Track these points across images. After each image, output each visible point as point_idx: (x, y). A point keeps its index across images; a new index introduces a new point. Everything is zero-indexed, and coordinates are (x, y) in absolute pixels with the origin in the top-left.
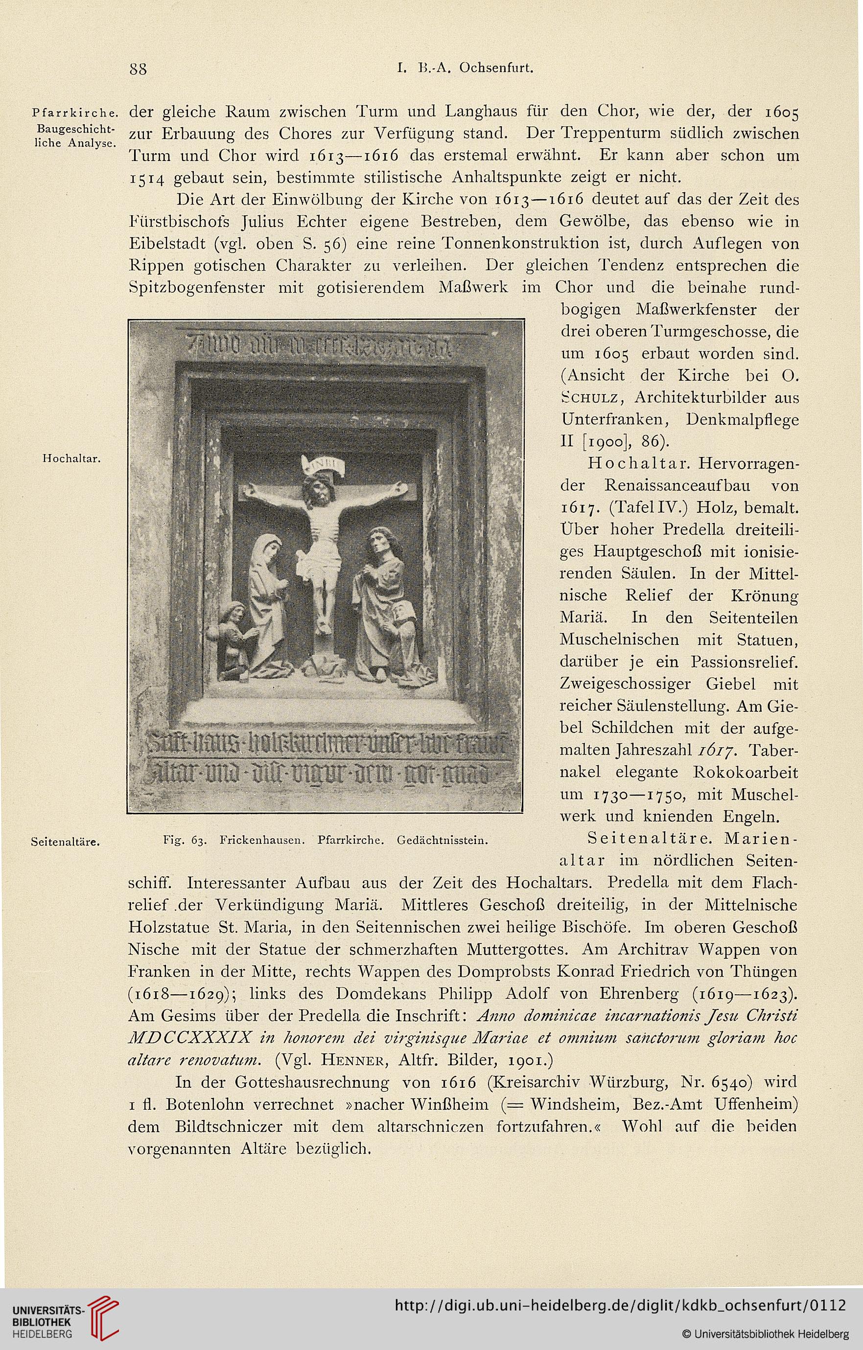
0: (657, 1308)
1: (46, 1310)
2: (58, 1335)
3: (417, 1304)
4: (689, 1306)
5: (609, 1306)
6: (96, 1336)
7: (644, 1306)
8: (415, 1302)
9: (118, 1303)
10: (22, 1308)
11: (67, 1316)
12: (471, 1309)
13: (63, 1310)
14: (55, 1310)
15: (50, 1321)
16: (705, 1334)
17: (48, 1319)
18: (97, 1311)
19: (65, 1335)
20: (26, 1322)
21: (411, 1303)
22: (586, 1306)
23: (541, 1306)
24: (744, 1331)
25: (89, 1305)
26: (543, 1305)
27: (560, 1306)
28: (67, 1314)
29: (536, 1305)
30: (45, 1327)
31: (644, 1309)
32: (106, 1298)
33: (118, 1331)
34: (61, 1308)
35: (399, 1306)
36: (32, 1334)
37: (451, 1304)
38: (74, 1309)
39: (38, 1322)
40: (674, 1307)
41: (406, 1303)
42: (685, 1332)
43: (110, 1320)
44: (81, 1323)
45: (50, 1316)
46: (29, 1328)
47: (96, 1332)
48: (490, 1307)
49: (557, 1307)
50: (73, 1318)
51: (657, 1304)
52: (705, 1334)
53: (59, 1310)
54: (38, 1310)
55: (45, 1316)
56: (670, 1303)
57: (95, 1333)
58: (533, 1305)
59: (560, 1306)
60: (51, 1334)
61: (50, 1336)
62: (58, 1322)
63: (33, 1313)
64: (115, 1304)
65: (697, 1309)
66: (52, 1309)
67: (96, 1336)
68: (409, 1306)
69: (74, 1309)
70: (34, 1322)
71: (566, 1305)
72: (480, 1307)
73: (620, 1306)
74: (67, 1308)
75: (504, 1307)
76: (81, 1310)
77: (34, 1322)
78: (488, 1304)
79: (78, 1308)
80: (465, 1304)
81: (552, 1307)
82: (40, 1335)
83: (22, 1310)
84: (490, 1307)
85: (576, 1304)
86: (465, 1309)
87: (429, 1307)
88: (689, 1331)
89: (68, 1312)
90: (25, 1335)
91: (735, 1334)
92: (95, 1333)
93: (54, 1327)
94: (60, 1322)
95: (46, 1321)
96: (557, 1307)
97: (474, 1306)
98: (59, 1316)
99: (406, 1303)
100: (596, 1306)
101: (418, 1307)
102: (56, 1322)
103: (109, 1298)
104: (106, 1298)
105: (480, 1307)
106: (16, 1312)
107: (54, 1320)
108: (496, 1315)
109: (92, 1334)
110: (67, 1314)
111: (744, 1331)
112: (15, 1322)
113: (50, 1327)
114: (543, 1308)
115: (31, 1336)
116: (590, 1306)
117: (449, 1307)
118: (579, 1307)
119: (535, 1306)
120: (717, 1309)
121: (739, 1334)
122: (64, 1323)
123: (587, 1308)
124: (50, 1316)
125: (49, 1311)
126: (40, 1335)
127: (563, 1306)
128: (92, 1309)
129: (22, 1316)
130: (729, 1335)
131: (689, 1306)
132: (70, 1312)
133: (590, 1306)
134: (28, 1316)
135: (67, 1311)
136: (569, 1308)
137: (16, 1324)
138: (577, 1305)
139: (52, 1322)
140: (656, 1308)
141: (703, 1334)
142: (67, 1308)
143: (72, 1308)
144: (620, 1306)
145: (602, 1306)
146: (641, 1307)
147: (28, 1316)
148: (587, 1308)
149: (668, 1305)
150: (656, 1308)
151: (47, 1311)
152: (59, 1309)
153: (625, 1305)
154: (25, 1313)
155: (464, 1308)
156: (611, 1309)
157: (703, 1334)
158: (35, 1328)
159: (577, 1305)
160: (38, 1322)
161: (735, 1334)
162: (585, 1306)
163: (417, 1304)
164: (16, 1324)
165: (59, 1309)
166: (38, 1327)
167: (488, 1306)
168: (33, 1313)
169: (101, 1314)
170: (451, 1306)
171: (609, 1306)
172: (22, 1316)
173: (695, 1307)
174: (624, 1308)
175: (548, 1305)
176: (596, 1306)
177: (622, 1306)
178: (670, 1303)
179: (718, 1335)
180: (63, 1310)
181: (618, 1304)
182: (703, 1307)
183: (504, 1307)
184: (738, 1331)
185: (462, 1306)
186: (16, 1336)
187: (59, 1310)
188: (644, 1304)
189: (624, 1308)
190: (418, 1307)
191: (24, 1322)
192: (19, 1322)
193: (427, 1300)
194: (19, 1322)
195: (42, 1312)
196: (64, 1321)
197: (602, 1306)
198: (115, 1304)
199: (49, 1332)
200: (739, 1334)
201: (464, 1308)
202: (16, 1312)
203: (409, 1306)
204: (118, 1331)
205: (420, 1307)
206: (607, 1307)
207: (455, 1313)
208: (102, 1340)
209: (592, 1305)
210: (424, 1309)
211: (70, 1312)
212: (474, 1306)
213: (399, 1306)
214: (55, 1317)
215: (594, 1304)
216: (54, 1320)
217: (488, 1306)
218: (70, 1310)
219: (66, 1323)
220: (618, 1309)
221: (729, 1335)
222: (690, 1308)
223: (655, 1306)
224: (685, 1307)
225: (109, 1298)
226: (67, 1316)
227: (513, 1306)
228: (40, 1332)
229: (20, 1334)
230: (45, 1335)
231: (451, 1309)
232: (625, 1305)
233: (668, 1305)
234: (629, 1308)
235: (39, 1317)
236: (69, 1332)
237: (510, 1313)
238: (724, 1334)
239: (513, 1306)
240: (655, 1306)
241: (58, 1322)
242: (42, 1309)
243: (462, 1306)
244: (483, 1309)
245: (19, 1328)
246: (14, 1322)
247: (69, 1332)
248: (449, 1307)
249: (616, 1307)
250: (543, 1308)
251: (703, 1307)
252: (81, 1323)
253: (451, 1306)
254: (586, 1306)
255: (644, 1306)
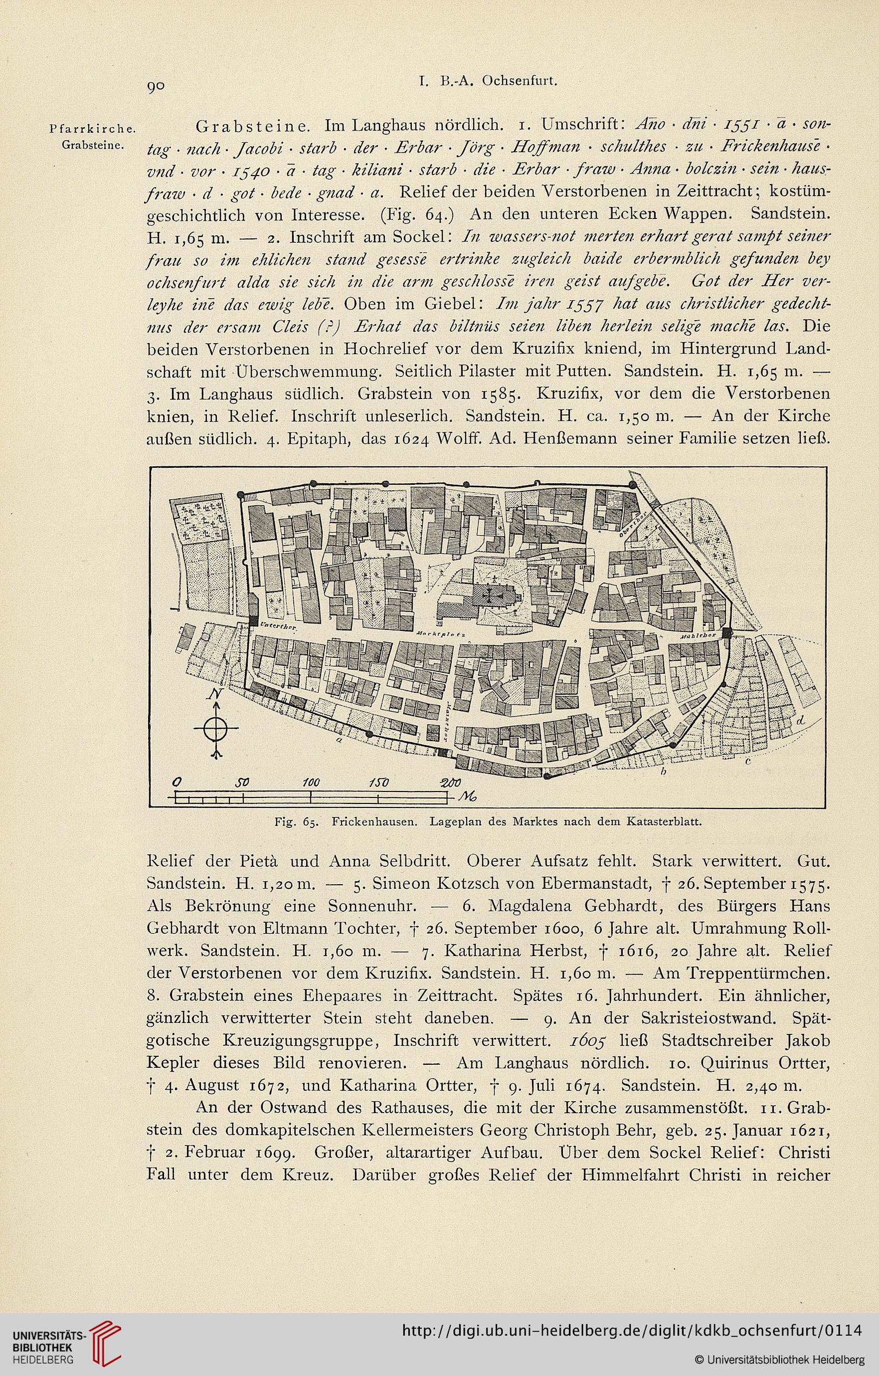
0: (670, 1334)
1: (46, 1335)
2: (59, 1361)
3: (425, 1329)
4: (702, 1332)
5: (620, 1331)
6: (98, 1362)
7: (656, 1331)
8: (423, 1327)
9: (120, 1329)
10: (22, 1333)
11: (68, 1341)
12: (480, 1334)
13: (65, 1335)
14: (56, 1335)
15: (51, 1347)
16: (718, 1360)
17: (49, 1345)
18: (99, 1336)
19: (66, 1360)
20: (27, 1348)
21: (419, 1328)
22: (597, 1331)
23: (551, 1331)
24: (758, 1357)
25: (90, 1330)
26: (553, 1330)
27: (570, 1331)
28: (68, 1339)
29: (546, 1330)
30: (46, 1352)
31: (656, 1334)
32: (108, 1323)
33: (120, 1357)
34: (62, 1333)
35: (407, 1331)
36: (33, 1360)
37: (460, 1329)
38: (76, 1334)
39: (38, 1347)
40: (686, 1332)
41: (413, 1328)
42: (697, 1357)
43: (112, 1346)
44: (82, 1349)
45: (50, 1342)
46: (29, 1353)
47: (98, 1358)
48: (499, 1332)
49: (567, 1332)
50: (74, 1343)
51: (670, 1329)
52: (718, 1360)
53: (60, 1335)
54: (39, 1336)
55: (46, 1341)
56: (683, 1328)
57: (96, 1359)
58: (543, 1330)
59: (570, 1331)
60: (52, 1360)
61: (50, 1361)
62: (59, 1348)
63: (34, 1338)
64: (117, 1329)
65: (710, 1334)
66: (53, 1335)
67: (98, 1362)
68: (416, 1331)
69: (76, 1334)
70: (34, 1348)
71: (576, 1330)
72: (489, 1333)
73: (631, 1331)
74: (68, 1333)
75: (513, 1333)
76: (83, 1335)
77: (34, 1348)
78: (497, 1329)
79: (79, 1333)
80: (474, 1329)
81: (562, 1332)
82: (41, 1361)
83: (23, 1335)
84: (499, 1332)
85: (587, 1329)
86: (474, 1334)
87: (437, 1332)
88: (701, 1357)
89: (70, 1337)
90: (25, 1361)
91: (749, 1360)
92: (96, 1359)
93: (55, 1353)
94: (61, 1348)
95: (47, 1346)
96: (567, 1332)
97: (482, 1331)
98: (60, 1341)
99: (413, 1328)
100: (608, 1331)
101: (426, 1332)
102: (57, 1348)
103: (111, 1323)
104: (108, 1323)
105: (489, 1333)
106: (16, 1337)
107: (55, 1346)
108: (505, 1340)
109: (94, 1360)
110: (68, 1339)
111: (758, 1357)
112: (15, 1348)
113: (51, 1353)
114: (554, 1333)
115: (32, 1361)
116: (601, 1331)
117: (457, 1332)
118: (590, 1332)
119: (545, 1331)
120: (730, 1335)
121: (753, 1360)
122: (65, 1349)
123: (598, 1333)
124: (50, 1342)
125: (50, 1336)
126: (41, 1361)
127: (574, 1331)
128: (94, 1334)
129: (23, 1341)
130: (742, 1361)
131: (702, 1332)
132: (72, 1337)
133: (601, 1331)
134: (28, 1342)
135: (68, 1337)
136: (580, 1333)
137: (16, 1349)
138: (588, 1330)
139: (53, 1348)
140: (668, 1333)
141: (716, 1360)
142: (68, 1333)
143: (74, 1333)
144: (631, 1331)
145: (613, 1332)
146: (653, 1332)
147: (28, 1342)
148: (598, 1333)
149: (681, 1330)
150: (668, 1333)
151: (47, 1336)
152: (60, 1335)
153: (637, 1330)
154: (26, 1338)
155: (472, 1333)
156: (623, 1334)
157: (716, 1360)
158: (35, 1354)
159: (588, 1330)
160: (38, 1347)
161: (749, 1360)
162: (596, 1331)
163: (425, 1329)
164: (16, 1349)
165: (60, 1335)
166: (39, 1353)
167: (497, 1331)
168: (34, 1338)
169: (103, 1339)
170: (459, 1331)
171: (620, 1331)
172: (23, 1341)
173: (707, 1332)
174: (636, 1333)
175: (558, 1330)
176: (608, 1331)
177: (634, 1332)
178: (683, 1328)
179: (731, 1360)
180: (65, 1335)
181: (630, 1329)
182: (716, 1332)
183: (513, 1333)
184: (752, 1357)
185: (471, 1332)
186: (16, 1361)
187: (60, 1335)
188: (656, 1329)
189: (636, 1333)
190: (426, 1332)
191: (25, 1348)
192: (20, 1347)
193: (435, 1325)
194: (20, 1347)
195: (42, 1337)
196: (65, 1346)
197: (613, 1332)
198: (117, 1329)
199: (50, 1358)
200: (753, 1360)
201: (472, 1333)
202: (16, 1337)
203: (416, 1331)
204: (120, 1357)
205: (427, 1332)
206: (619, 1332)
207: (464, 1338)
208: (104, 1366)
209: (603, 1330)
210: (432, 1334)
211: (72, 1337)
212: (482, 1331)
213: (407, 1331)
214: (56, 1342)
215: (605, 1329)
216: (55, 1346)
217: (497, 1331)
218: (71, 1335)
219: (67, 1348)
220: (630, 1334)
221: (742, 1361)
222: (703, 1333)
223: (667, 1332)
224: (697, 1332)
225: (111, 1323)
226: (68, 1341)
227: (523, 1331)
228: (41, 1358)
229: (20, 1360)
230: (46, 1360)
231: (460, 1334)
232: (637, 1330)
233: (681, 1330)
234: (641, 1333)
235: (40, 1342)
236: (70, 1358)
237: (520, 1339)
238: (738, 1360)
239: (523, 1331)
240: (667, 1332)
241: (59, 1348)
242: (43, 1334)
243: (471, 1332)
244: (492, 1334)
245: (20, 1353)
246: (14, 1348)
247: (70, 1358)
248: (457, 1332)
249: (627, 1332)
250: (554, 1333)
251: (716, 1332)
252: (82, 1349)
253: (459, 1331)
254: (597, 1331)
255: (656, 1331)
